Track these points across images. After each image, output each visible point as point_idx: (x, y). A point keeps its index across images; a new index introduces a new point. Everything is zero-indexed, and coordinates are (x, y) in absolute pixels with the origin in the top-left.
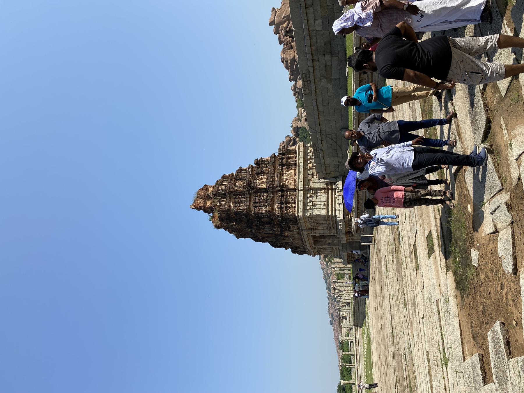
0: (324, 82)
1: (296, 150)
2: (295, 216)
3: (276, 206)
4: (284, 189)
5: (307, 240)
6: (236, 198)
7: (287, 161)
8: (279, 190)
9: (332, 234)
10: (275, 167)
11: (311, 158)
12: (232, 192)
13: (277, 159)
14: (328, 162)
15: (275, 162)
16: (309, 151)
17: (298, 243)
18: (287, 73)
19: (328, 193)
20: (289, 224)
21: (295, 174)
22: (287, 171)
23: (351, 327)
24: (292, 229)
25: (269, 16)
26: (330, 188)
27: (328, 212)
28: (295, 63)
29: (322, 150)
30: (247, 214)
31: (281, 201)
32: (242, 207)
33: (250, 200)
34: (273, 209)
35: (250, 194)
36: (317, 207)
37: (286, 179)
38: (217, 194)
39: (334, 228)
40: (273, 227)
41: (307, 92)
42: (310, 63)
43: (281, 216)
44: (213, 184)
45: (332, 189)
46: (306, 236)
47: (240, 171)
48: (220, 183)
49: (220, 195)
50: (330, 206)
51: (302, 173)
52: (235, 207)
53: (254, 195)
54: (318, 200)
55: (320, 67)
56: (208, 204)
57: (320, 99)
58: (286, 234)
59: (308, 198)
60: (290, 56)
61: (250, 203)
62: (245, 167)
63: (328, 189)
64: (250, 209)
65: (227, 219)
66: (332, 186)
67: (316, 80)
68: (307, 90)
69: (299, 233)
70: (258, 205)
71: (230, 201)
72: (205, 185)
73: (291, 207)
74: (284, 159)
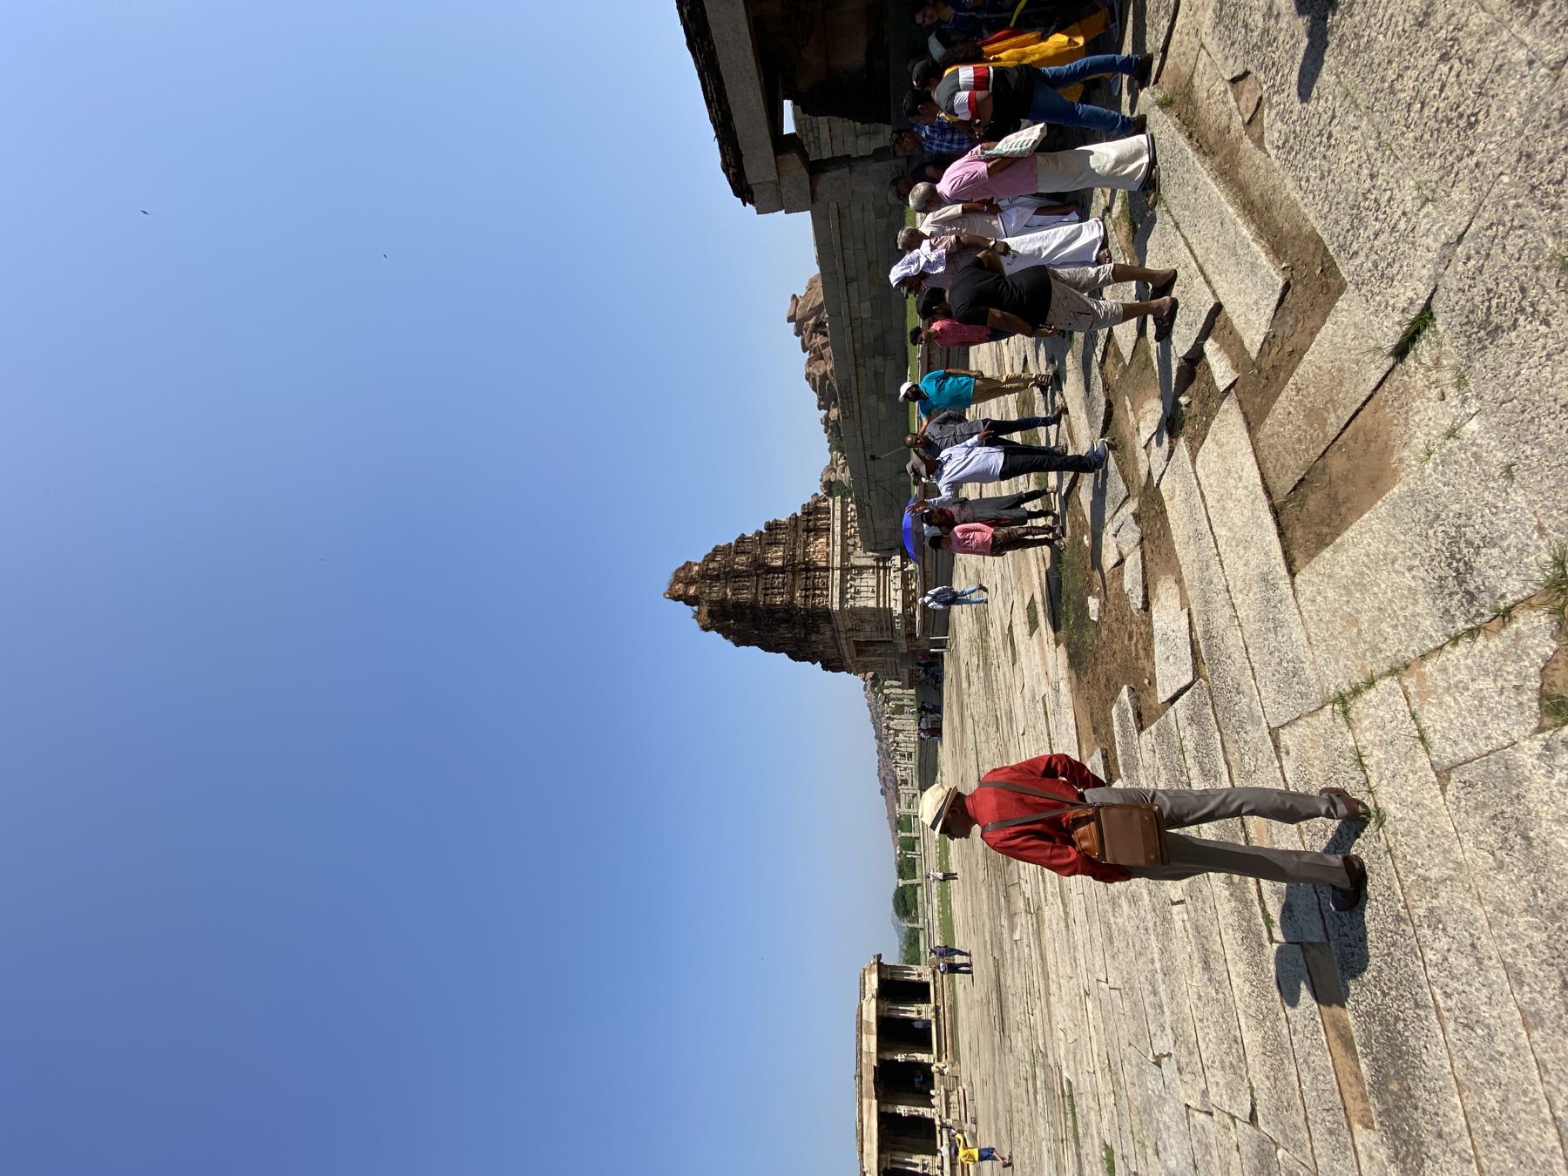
0: (872, 399)
4: (810, 568)
14: (879, 525)
18: (815, 397)
25: (786, 308)
26: (882, 566)
30: (753, 606)
32: (745, 596)
34: (793, 597)
38: (706, 576)
42: (852, 370)
44: (700, 560)
45: (885, 568)
48: (710, 558)
49: (711, 577)
56: (692, 591)
57: (866, 426)
64: (759, 600)
69: (833, 637)
74: (811, 521)
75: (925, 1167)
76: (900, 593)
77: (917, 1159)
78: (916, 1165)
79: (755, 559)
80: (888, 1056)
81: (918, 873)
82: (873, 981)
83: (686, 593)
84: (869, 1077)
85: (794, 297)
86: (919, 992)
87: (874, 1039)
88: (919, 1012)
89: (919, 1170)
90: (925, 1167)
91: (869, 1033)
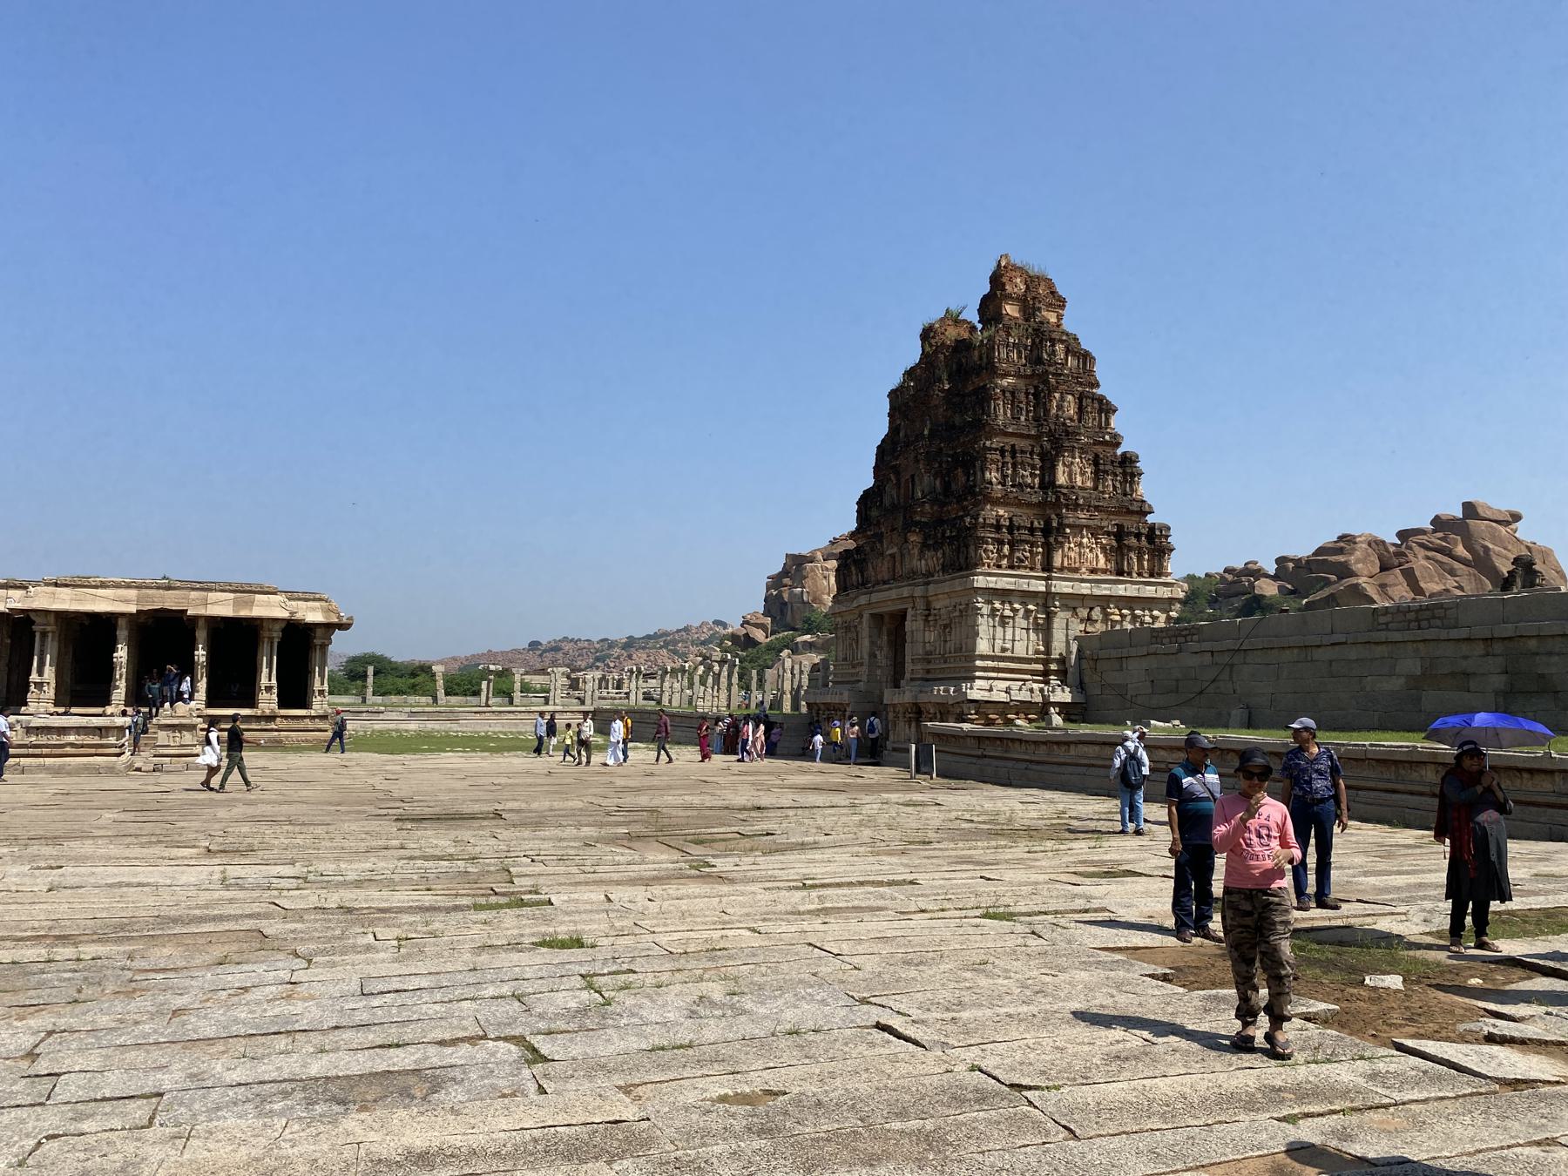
0: (1411, 665)
1: (1160, 575)
2: (976, 565)
3: (1001, 512)
5: (893, 594)
6: (1027, 394)
7: (1130, 549)
8: (1048, 522)
9: (909, 666)
10: (1113, 513)
11: (1134, 618)
12: (1046, 382)
13: (1135, 518)
15: (1130, 512)
16: (1156, 613)
17: (881, 568)
19: (1036, 661)
20: (946, 548)
21: (1093, 571)
22: (1103, 549)
23: (588, 701)
24: (928, 554)
26: (1049, 667)
27: (983, 658)
28: (1333, 577)
29: (1180, 651)
30: (981, 427)
31: (1019, 528)
32: (1001, 413)
33: (1021, 436)
34: (996, 502)
35: (1038, 438)
36: (999, 630)
37: (1080, 545)
38: (1041, 338)
39: (928, 671)
40: (933, 502)
41: (1382, 619)
43: (975, 526)
44: (1068, 325)
45: (1046, 673)
46: (906, 592)
47: (1106, 408)
48: (1073, 347)
49: (1037, 347)
50: (1002, 665)
51: (1097, 592)
52: (1003, 391)
53: (1037, 450)
54: (1018, 631)
55: (1466, 658)
56: (1011, 310)
57: (1353, 653)
58: (913, 538)
59: (1024, 604)
60: (1358, 561)
61: (1012, 435)
62: (1116, 422)
63: (1046, 662)
64: (984, 433)
65: (960, 365)
66: (1055, 673)
67: (1421, 646)
68: (1388, 618)
69: (913, 574)
70: (1008, 459)
71: (1018, 375)
72: (1064, 301)
73: (1001, 557)
74: (1139, 542)
75: (39, 685)
76: (1003, 697)
77: (49, 673)
78: (40, 673)
79: (1070, 434)
80: (201, 635)
81: (454, 699)
82: (312, 614)
84: (170, 601)
85: (1516, 517)
86: (294, 693)
87: (227, 611)
88: (269, 689)
89: (34, 677)
90: (39, 685)
91: (236, 603)
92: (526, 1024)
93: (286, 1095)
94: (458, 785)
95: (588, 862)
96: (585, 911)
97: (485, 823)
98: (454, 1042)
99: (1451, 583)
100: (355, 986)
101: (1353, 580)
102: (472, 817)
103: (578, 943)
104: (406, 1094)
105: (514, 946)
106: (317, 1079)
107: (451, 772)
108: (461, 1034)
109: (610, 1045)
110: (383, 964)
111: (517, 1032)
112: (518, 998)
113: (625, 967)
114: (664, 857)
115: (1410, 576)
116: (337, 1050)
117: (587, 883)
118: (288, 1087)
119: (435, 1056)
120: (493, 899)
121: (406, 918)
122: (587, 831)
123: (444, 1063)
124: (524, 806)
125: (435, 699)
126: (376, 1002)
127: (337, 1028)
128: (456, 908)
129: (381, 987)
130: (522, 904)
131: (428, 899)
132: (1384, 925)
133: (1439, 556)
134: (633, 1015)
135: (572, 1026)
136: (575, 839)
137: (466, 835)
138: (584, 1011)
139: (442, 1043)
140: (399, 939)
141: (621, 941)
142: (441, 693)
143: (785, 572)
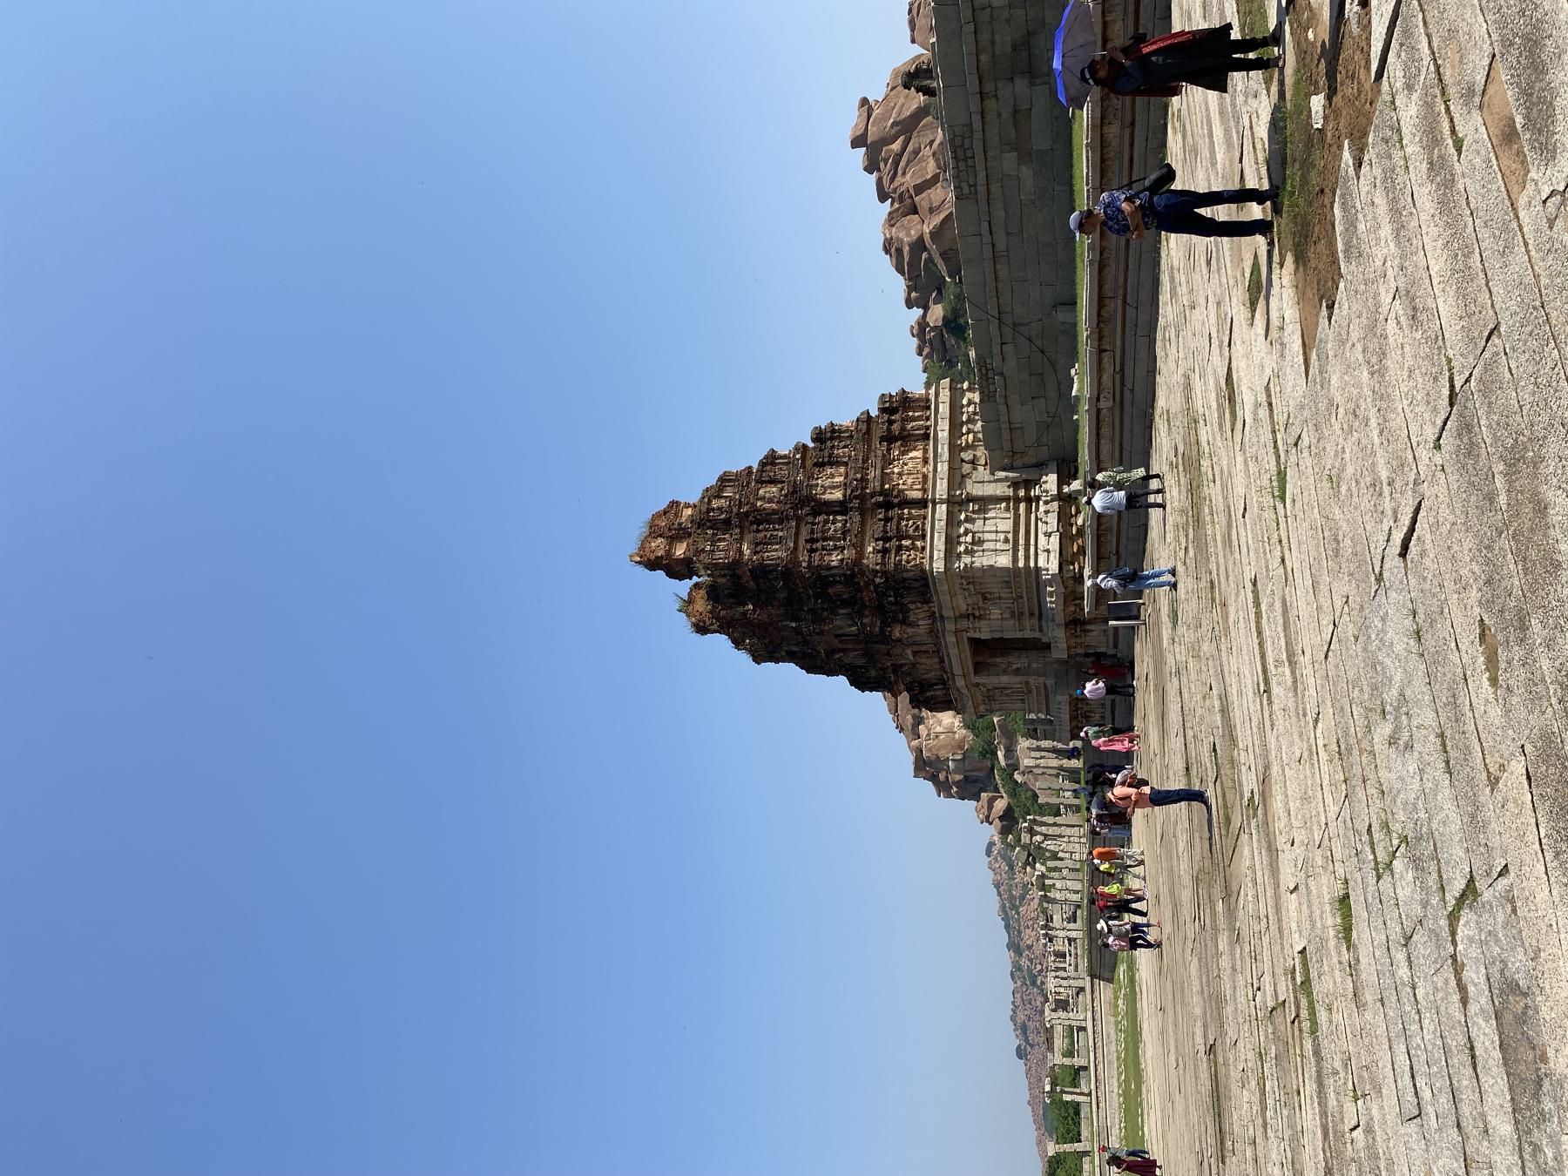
0: (1009, 161)
1: (928, 400)
2: (923, 571)
3: (870, 549)
4: (892, 502)
5: (953, 652)
6: (758, 531)
7: (903, 429)
8: (879, 505)
9: (1028, 634)
10: (869, 449)
11: (970, 421)
12: (747, 514)
13: (874, 426)
14: (1019, 415)
15: (868, 431)
16: (965, 402)
17: (928, 667)
18: (899, 284)
19: (1016, 509)
20: (906, 600)
21: (925, 461)
22: (903, 453)
23: (1080, 983)
24: (912, 618)
25: (850, 120)
26: (1023, 496)
27: (1015, 559)
28: (925, 255)
29: (1001, 374)
30: (788, 572)
31: (885, 532)
32: (776, 554)
33: (797, 534)
34: (861, 554)
35: (799, 519)
36: (986, 546)
37: (900, 474)
38: (708, 521)
39: (1032, 614)
40: (861, 615)
41: (966, 190)
42: (974, 105)
43: (884, 573)
44: (694, 498)
45: (1029, 500)
46: (951, 639)
47: (771, 459)
49: (714, 525)
50: (1022, 541)
51: (946, 456)
52: (756, 553)
53: (810, 519)
54: (987, 528)
55: (999, 115)
56: (680, 551)
57: (999, 213)
58: (897, 634)
59: (960, 523)
60: (908, 234)
61: (796, 543)
62: (784, 450)
63: (1017, 500)
64: (796, 573)
65: (730, 596)
66: (1028, 491)
67: (990, 154)
68: (965, 186)
69: (933, 632)
70: (819, 545)
71: (740, 541)
72: (673, 502)
73: (914, 547)
74: (897, 421)
76: (1055, 539)
79: (795, 490)
81: (1085, 1133)
83: (669, 553)
85: (864, 101)
92: (1436, 920)
93: (1537, 1149)
94: (1180, 1106)
95: (1257, 928)
96: (1309, 907)
97: (1221, 1060)
98: (1462, 988)
99: (927, 152)
100: (1412, 1127)
101: (927, 237)
102: (1215, 1078)
103: (1344, 901)
104: (1522, 1019)
105: (1353, 968)
106: (1517, 1122)
107: (1167, 1119)
108: (1453, 983)
109: (1449, 818)
110: (1384, 1109)
111: (1443, 922)
112: (1408, 938)
113: (1365, 838)
114: (1246, 852)
115: (920, 188)
116: (1483, 1115)
117: (1280, 920)
118: (1528, 1149)
119: (1480, 1000)
120: (1304, 1014)
121: (1332, 1102)
122: (1223, 943)
123: (1486, 988)
124: (1199, 1024)
125: (1086, 1153)
126: (1426, 1094)
127: (1459, 1126)
128: (1317, 1053)
129: (1410, 1096)
130: (1307, 982)
131: (1310, 1088)
132: (1262, 131)
133: (902, 164)
134: (1415, 808)
135: (1433, 867)
136: (1233, 955)
137: (1235, 1075)
138: (1416, 863)
139: (1464, 1001)
140: (1356, 1100)
141: (1338, 856)
142: (1078, 1147)
143: (933, 778)
